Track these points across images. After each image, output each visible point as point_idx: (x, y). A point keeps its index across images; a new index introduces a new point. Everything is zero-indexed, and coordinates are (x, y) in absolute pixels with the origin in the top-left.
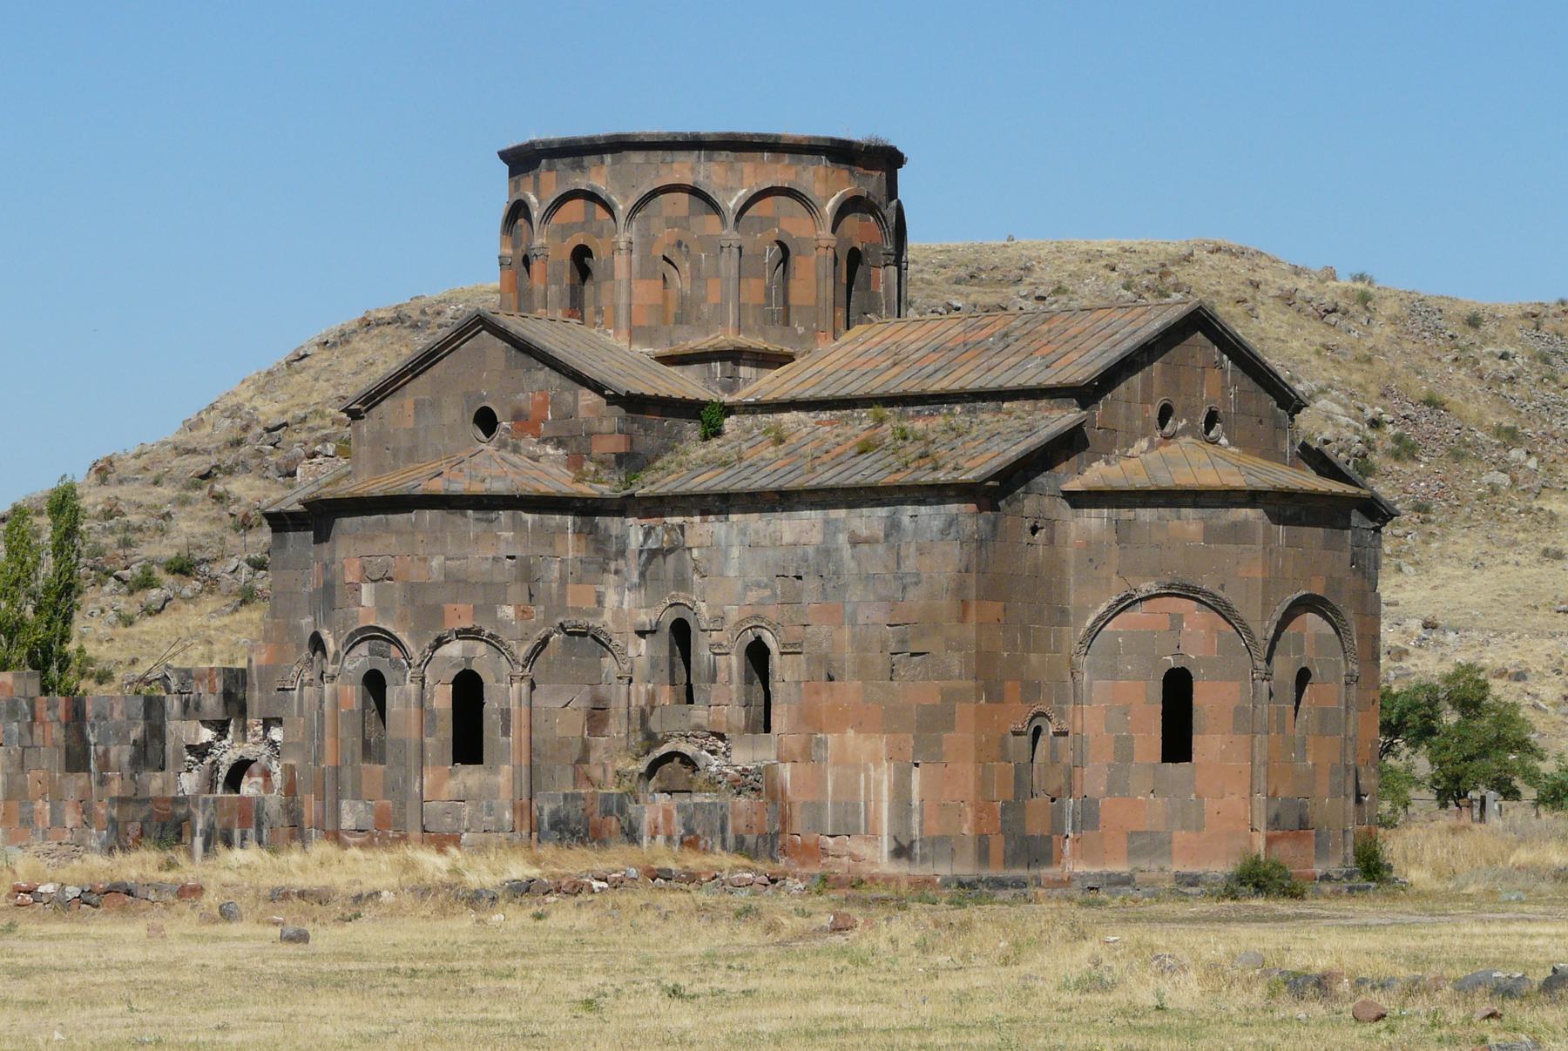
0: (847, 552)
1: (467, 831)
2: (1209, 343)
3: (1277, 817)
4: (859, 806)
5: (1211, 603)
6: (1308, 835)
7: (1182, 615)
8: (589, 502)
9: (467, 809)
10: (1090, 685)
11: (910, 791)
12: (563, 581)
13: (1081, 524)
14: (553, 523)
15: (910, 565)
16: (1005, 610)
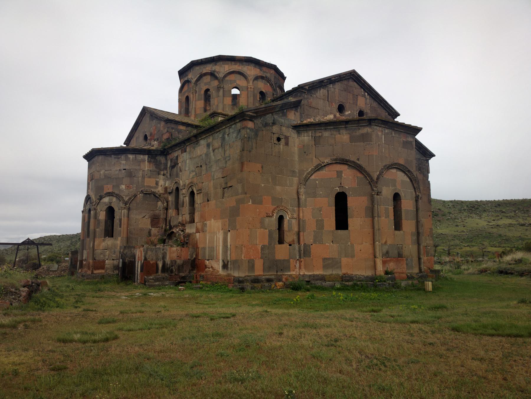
0: (212, 154)
1: (107, 259)
2: (359, 87)
3: (387, 252)
4: (214, 247)
5: (353, 165)
6: (403, 260)
7: (342, 171)
8: (152, 151)
9: (107, 253)
10: (306, 200)
11: (227, 241)
12: (143, 177)
13: (301, 139)
14: (140, 159)
15: (227, 153)
16: (262, 167)
